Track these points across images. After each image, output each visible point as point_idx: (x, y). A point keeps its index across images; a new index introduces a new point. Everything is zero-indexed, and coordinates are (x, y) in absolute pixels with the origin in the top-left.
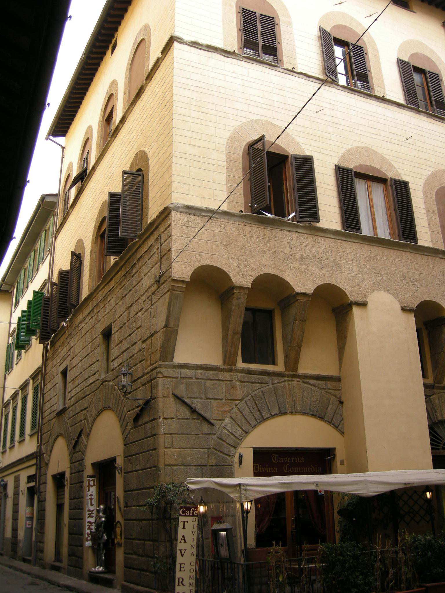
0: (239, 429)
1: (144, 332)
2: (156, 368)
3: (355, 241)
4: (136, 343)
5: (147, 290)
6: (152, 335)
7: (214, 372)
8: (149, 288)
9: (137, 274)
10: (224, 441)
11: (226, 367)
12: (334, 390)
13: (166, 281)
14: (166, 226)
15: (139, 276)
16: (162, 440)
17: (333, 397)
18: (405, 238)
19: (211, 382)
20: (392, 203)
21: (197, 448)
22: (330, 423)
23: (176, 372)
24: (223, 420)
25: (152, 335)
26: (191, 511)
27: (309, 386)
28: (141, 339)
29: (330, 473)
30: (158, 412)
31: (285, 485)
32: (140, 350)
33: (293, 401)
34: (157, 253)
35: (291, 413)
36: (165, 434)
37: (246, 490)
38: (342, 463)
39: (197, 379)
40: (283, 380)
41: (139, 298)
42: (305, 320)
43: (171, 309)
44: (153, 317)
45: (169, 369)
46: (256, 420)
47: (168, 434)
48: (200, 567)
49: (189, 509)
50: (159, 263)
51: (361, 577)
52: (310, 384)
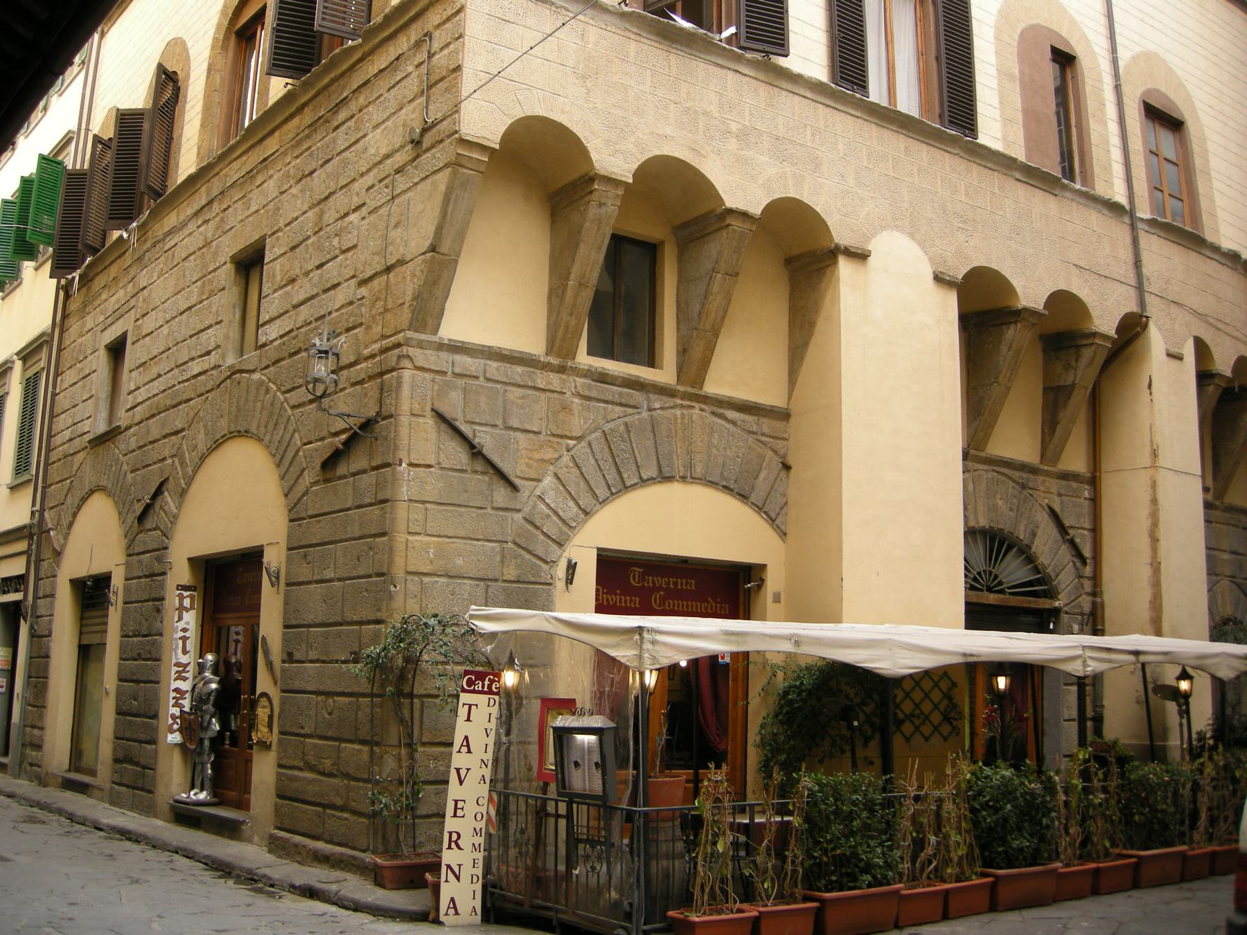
0: (571, 504)
1: (366, 260)
2: (398, 345)
3: (853, 112)
4: (339, 284)
5: (380, 162)
6: (389, 269)
7: (526, 369)
8: (387, 156)
9: (351, 123)
10: (537, 527)
11: (554, 361)
12: (773, 437)
13: (442, 141)
14: (449, 12)
15: (358, 129)
16: (402, 513)
17: (770, 454)
18: (953, 123)
19: (519, 392)
20: (933, 42)
21: (478, 540)
22: (759, 509)
23: (442, 360)
24: (539, 480)
25: (389, 269)
26: (487, 682)
27: (724, 423)
28: (354, 277)
29: (747, 617)
30: (396, 448)
31: (733, 638)
32: (351, 303)
33: (689, 452)
34: (415, 74)
35: (683, 479)
36: (411, 501)
37: (654, 642)
38: (777, 599)
39: (488, 380)
40: (672, 404)
41: (354, 180)
42: (737, 275)
43: (450, 209)
44: (396, 226)
45: (427, 352)
46: (609, 488)
47: (416, 501)
48: (498, 813)
49: (481, 676)
50: (422, 100)
51: (879, 850)
52: (726, 419)
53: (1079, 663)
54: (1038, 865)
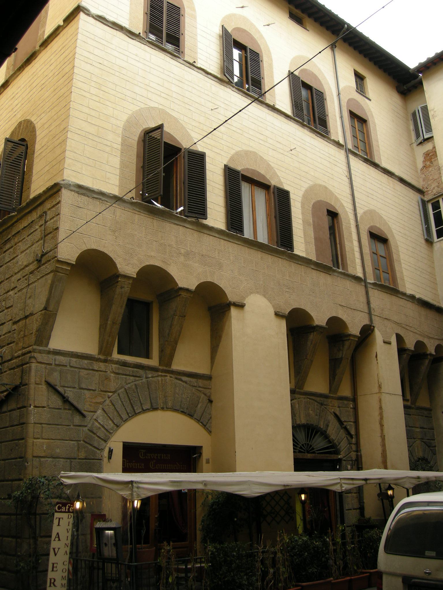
0: (110, 422)
1: (17, 312)
2: (30, 352)
3: (237, 242)
4: (4, 323)
5: (23, 269)
6: (26, 317)
7: (88, 361)
8: (26, 266)
9: (11, 250)
10: (94, 434)
11: (102, 357)
12: (205, 388)
13: (49, 261)
14: (54, 203)
15: (14, 253)
16: (31, 429)
17: (203, 396)
18: (282, 245)
19: (85, 372)
20: (273, 210)
21: (67, 440)
22: (198, 421)
23: (51, 358)
24: (95, 412)
25: (26, 317)
26: (67, 507)
27: (180, 382)
28: (11, 320)
29: (195, 471)
30: (28, 399)
31: (176, 484)
32: (10, 332)
33: (165, 397)
34: (39, 230)
35: (163, 409)
36: (35, 423)
37: (138, 488)
38: (208, 462)
39: (71, 367)
40: (156, 375)
41: (12, 276)
42: (185, 316)
43: (53, 291)
44: (30, 298)
45: (43, 355)
46: (128, 414)
47: (38, 423)
48: (73, 568)
49: (64, 505)
50: (42, 241)
51: (245, 577)
52: (182, 381)
53: (339, 486)
54: (322, 579)
